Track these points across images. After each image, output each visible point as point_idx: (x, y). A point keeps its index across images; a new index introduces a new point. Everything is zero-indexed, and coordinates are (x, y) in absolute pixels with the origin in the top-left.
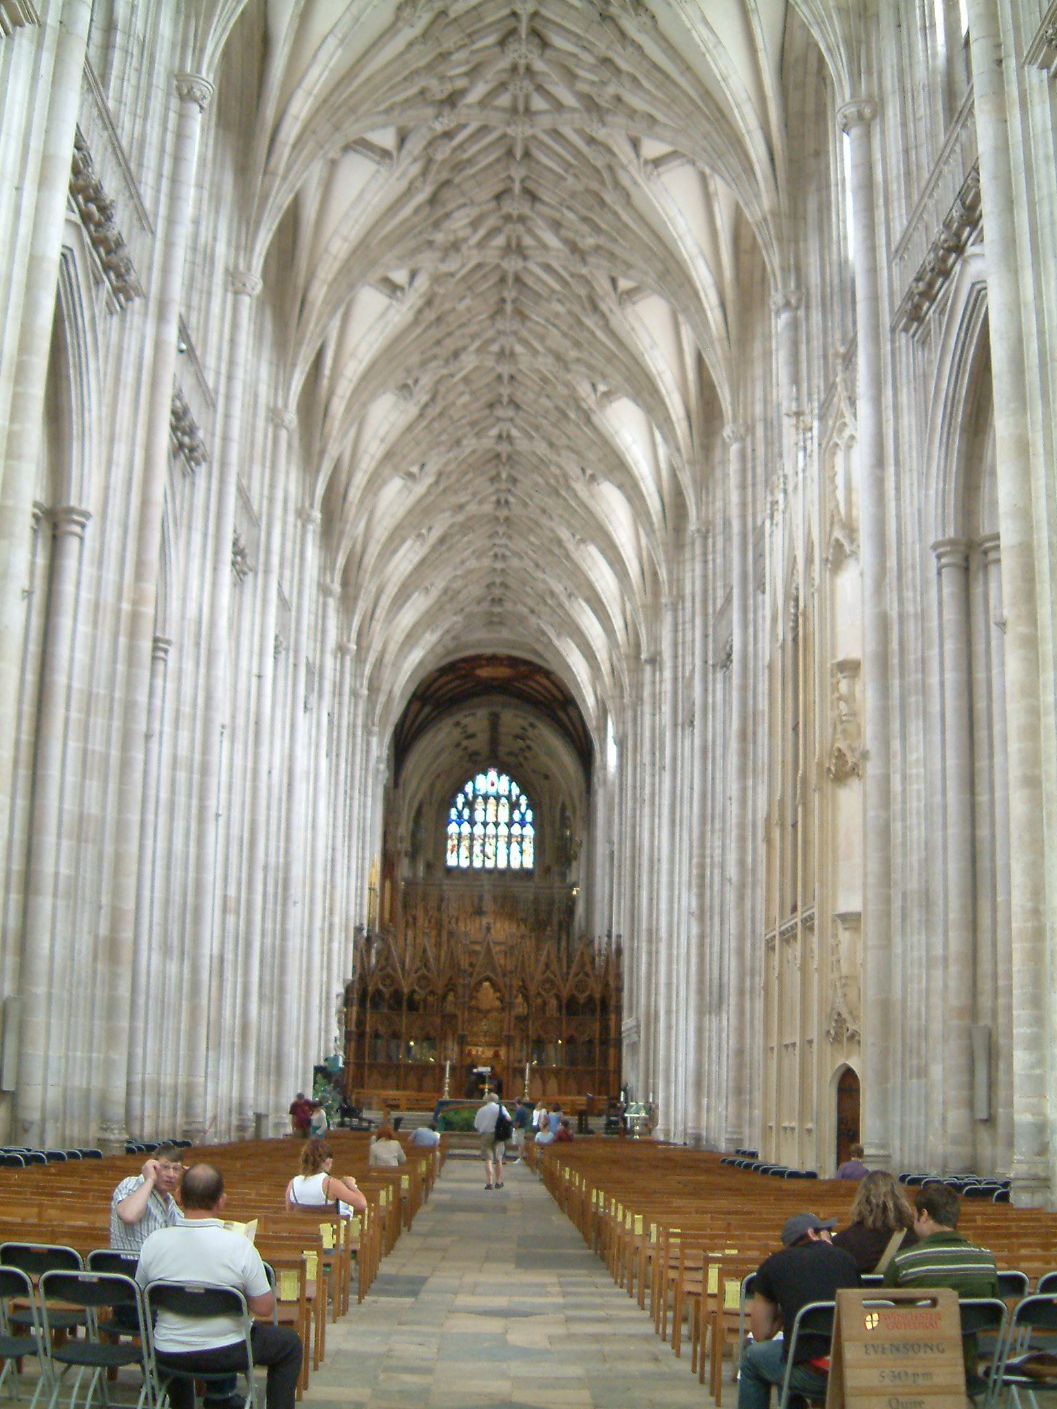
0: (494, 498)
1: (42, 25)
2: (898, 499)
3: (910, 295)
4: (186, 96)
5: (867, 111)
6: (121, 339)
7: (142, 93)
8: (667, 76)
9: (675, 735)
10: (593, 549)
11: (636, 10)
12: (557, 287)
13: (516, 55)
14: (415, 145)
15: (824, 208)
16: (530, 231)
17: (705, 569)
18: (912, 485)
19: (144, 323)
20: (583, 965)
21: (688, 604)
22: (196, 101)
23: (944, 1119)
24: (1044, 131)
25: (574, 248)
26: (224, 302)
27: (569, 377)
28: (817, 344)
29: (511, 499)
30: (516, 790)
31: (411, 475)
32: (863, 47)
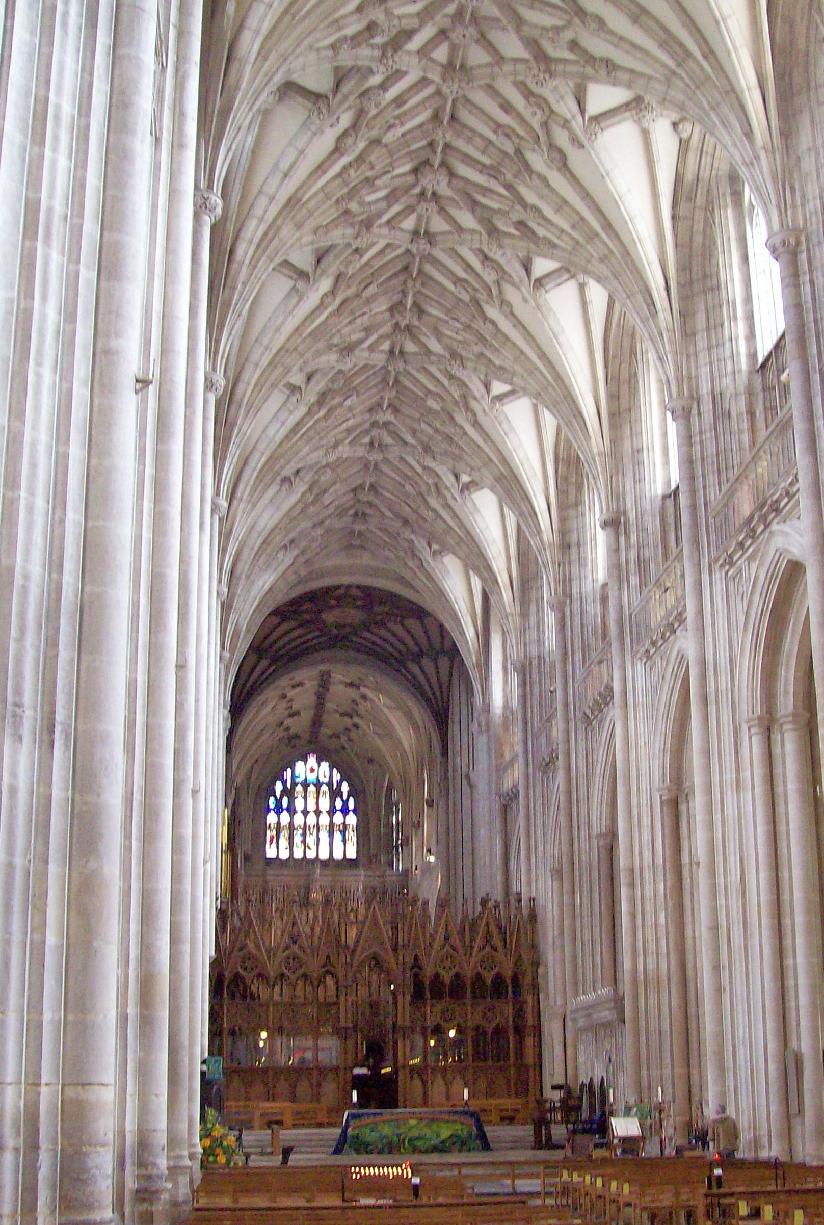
0: (386, 346)
20: (488, 939)
21: (707, 407)
29: (410, 347)
30: (337, 777)
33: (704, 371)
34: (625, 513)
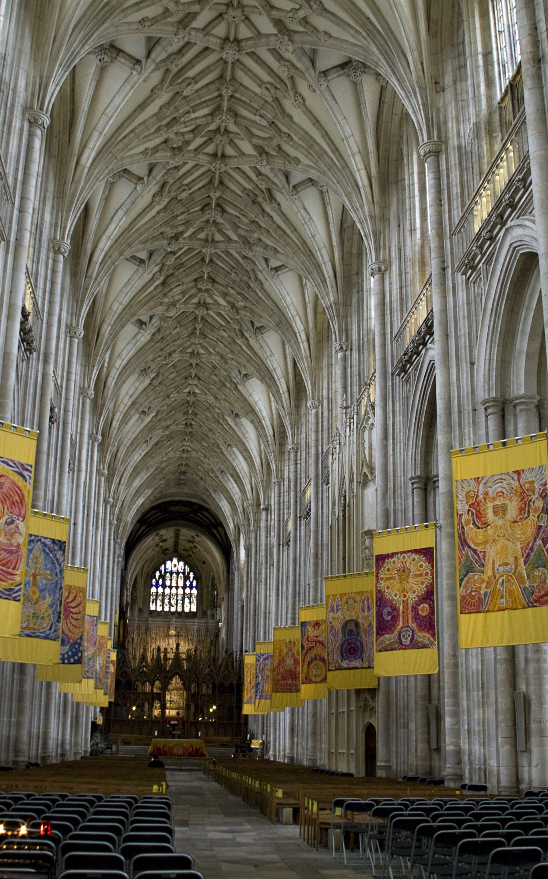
0: (184, 422)
1: (8, 242)
2: (394, 455)
3: (401, 361)
4: (57, 251)
5: (383, 268)
6: (27, 372)
7: (36, 250)
8: (285, 232)
9: (279, 550)
10: (235, 449)
11: (270, 201)
12: (223, 323)
13: (209, 216)
14: (157, 258)
15: (360, 301)
16: (211, 297)
17: (296, 468)
18: (400, 449)
19: (38, 364)
21: (286, 483)
22: (62, 253)
23: (416, 749)
24: (463, 304)
25: (233, 306)
26: (65, 341)
27: (227, 367)
28: (355, 369)
29: (193, 423)
30: (187, 570)
31: (143, 412)
32: (382, 235)
33: (286, 468)
34: (270, 506)
